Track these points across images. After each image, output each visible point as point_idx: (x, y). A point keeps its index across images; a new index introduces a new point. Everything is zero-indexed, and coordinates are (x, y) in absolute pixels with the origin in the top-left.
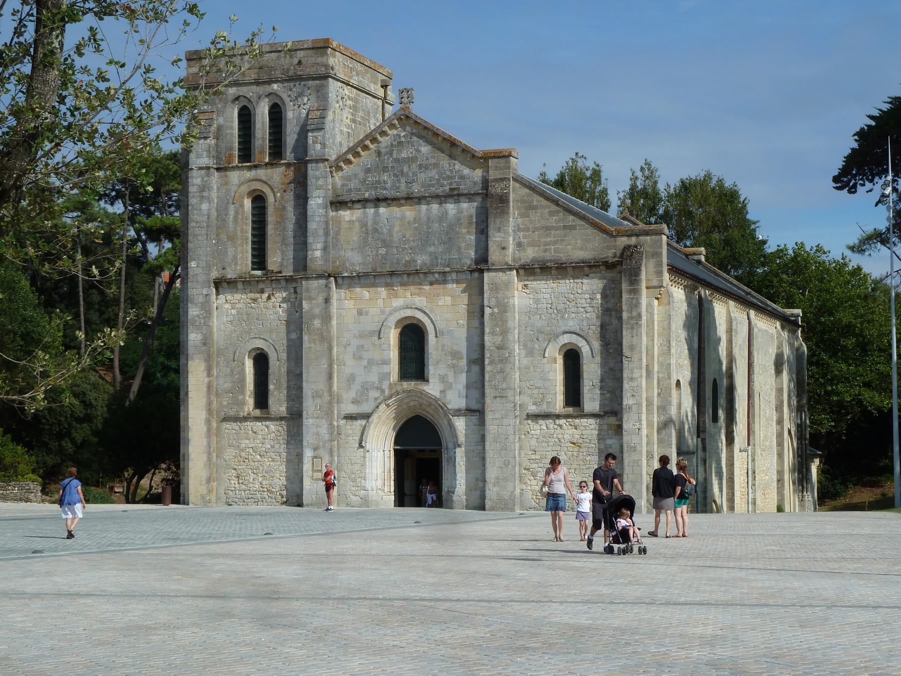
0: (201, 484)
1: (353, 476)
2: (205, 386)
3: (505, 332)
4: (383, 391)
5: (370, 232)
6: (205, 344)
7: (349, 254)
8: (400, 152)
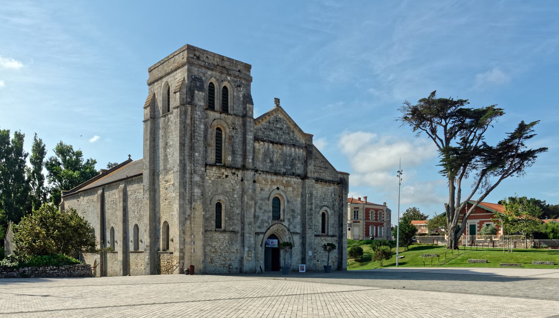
0: (200, 264)
1: (258, 259)
2: (202, 216)
3: (311, 204)
4: (269, 224)
5: (266, 154)
6: (202, 195)
7: (258, 163)
8: (276, 124)
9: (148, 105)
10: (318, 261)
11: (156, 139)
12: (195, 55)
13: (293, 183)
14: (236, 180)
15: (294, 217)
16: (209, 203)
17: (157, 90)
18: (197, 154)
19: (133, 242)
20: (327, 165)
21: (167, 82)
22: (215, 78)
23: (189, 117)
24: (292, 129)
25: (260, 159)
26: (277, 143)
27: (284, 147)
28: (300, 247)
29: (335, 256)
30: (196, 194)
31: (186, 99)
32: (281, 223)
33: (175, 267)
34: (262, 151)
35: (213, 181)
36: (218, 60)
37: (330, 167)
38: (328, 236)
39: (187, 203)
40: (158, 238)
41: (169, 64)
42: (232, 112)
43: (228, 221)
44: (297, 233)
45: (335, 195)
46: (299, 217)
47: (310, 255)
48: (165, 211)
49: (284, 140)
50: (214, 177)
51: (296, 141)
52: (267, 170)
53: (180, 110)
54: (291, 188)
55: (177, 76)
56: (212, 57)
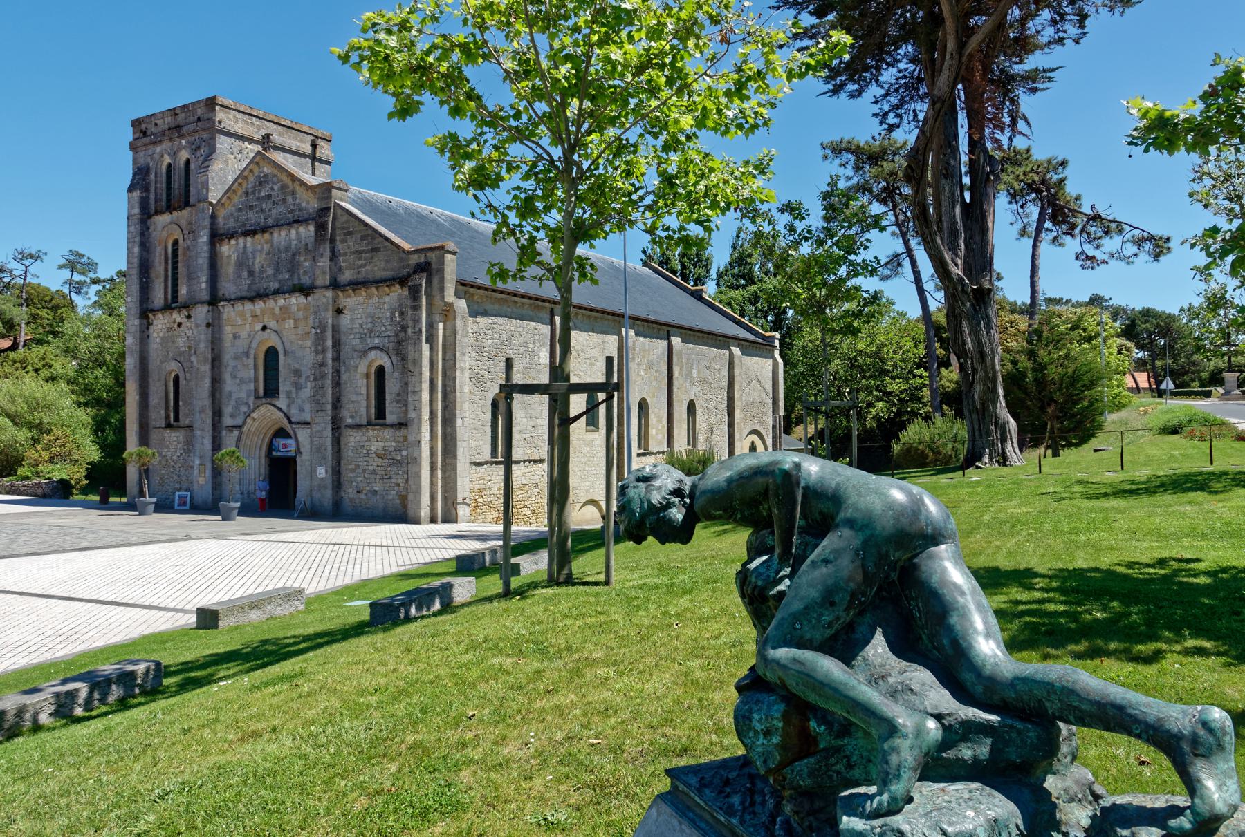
4: (249, 406)
7: (227, 285)
8: (260, 192)
10: (358, 492)
13: (294, 309)
15: (298, 387)
20: (376, 241)
24: (291, 188)
25: (231, 276)
32: (273, 402)
34: (234, 257)
35: (162, 338)
37: (387, 243)
38: (384, 425)
45: (402, 314)
51: (301, 210)
54: (292, 321)
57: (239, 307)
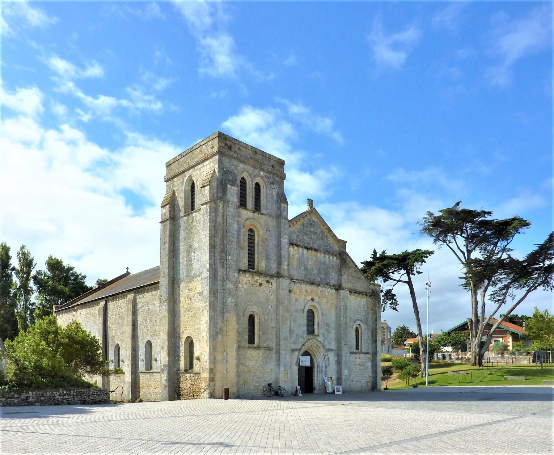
3: (346, 317)
4: (304, 339)
5: (300, 261)
6: (236, 305)
7: (292, 270)
8: (310, 228)
9: (166, 203)
10: (352, 381)
11: (176, 242)
12: (226, 145)
13: (327, 293)
14: (270, 288)
15: (328, 332)
16: (242, 314)
17: (177, 187)
18: (230, 258)
19: (145, 362)
21: (190, 176)
22: (247, 172)
23: (220, 215)
24: (326, 234)
25: (295, 267)
26: (311, 249)
27: (319, 254)
28: (335, 366)
29: (369, 376)
30: (229, 304)
31: (217, 194)
33: (203, 390)
34: (296, 257)
36: (251, 152)
38: (362, 353)
39: (219, 314)
40: (179, 357)
41: (194, 156)
42: (265, 212)
43: (262, 336)
44: (332, 350)
45: (367, 308)
46: (334, 332)
47: (346, 374)
48: (188, 324)
49: (318, 246)
50: (247, 284)
51: (330, 247)
52: (302, 278)
53: (210, 206)
54: (326, 299)
55: (204, 169)
56: (244, 149)
57: (298, 285)
